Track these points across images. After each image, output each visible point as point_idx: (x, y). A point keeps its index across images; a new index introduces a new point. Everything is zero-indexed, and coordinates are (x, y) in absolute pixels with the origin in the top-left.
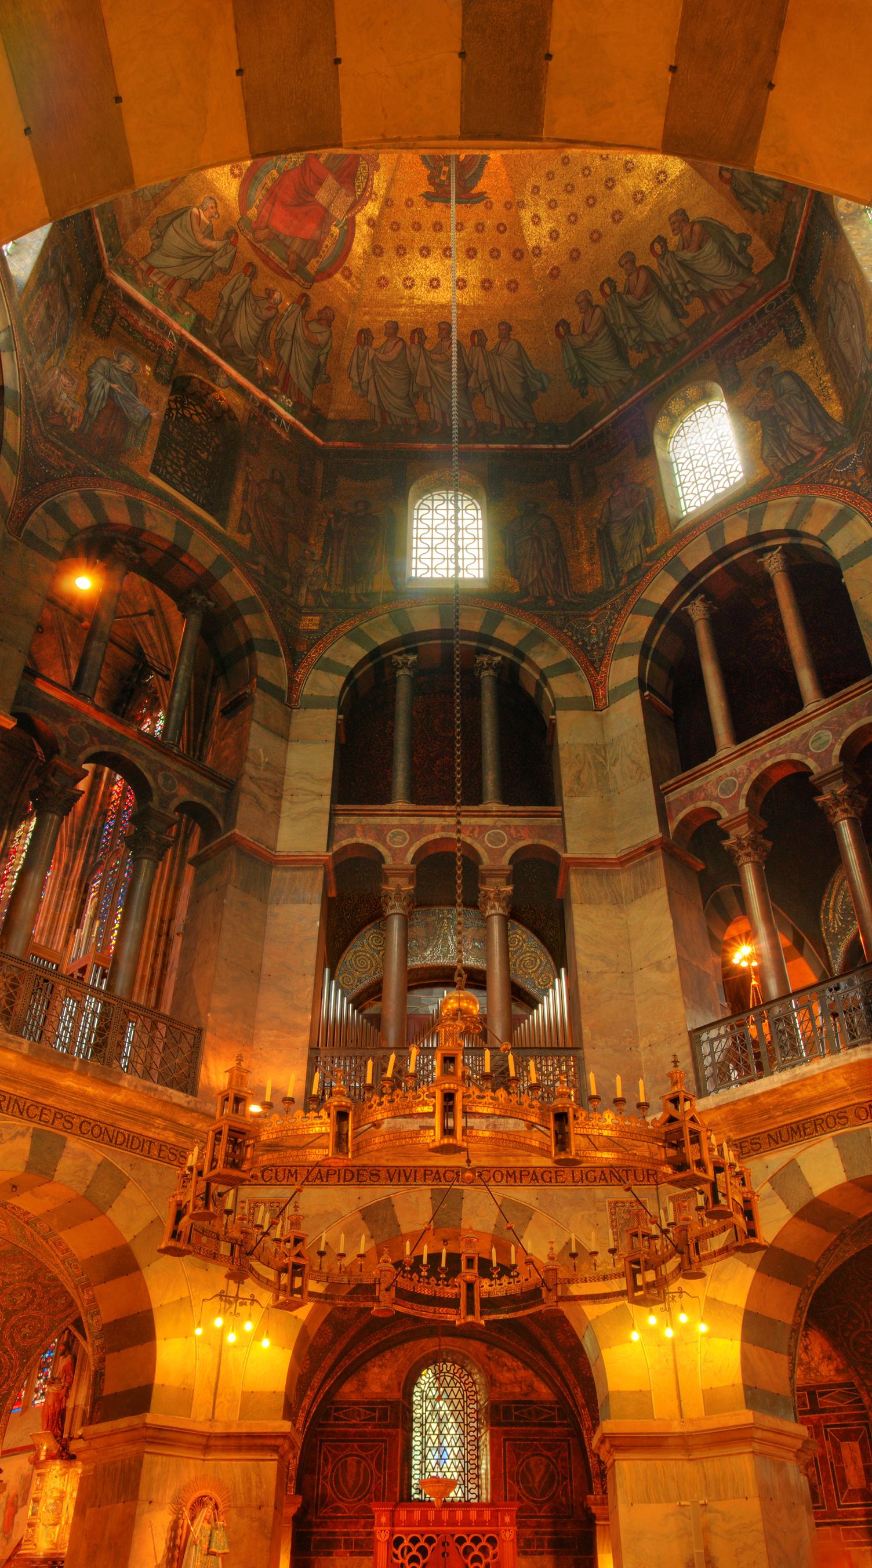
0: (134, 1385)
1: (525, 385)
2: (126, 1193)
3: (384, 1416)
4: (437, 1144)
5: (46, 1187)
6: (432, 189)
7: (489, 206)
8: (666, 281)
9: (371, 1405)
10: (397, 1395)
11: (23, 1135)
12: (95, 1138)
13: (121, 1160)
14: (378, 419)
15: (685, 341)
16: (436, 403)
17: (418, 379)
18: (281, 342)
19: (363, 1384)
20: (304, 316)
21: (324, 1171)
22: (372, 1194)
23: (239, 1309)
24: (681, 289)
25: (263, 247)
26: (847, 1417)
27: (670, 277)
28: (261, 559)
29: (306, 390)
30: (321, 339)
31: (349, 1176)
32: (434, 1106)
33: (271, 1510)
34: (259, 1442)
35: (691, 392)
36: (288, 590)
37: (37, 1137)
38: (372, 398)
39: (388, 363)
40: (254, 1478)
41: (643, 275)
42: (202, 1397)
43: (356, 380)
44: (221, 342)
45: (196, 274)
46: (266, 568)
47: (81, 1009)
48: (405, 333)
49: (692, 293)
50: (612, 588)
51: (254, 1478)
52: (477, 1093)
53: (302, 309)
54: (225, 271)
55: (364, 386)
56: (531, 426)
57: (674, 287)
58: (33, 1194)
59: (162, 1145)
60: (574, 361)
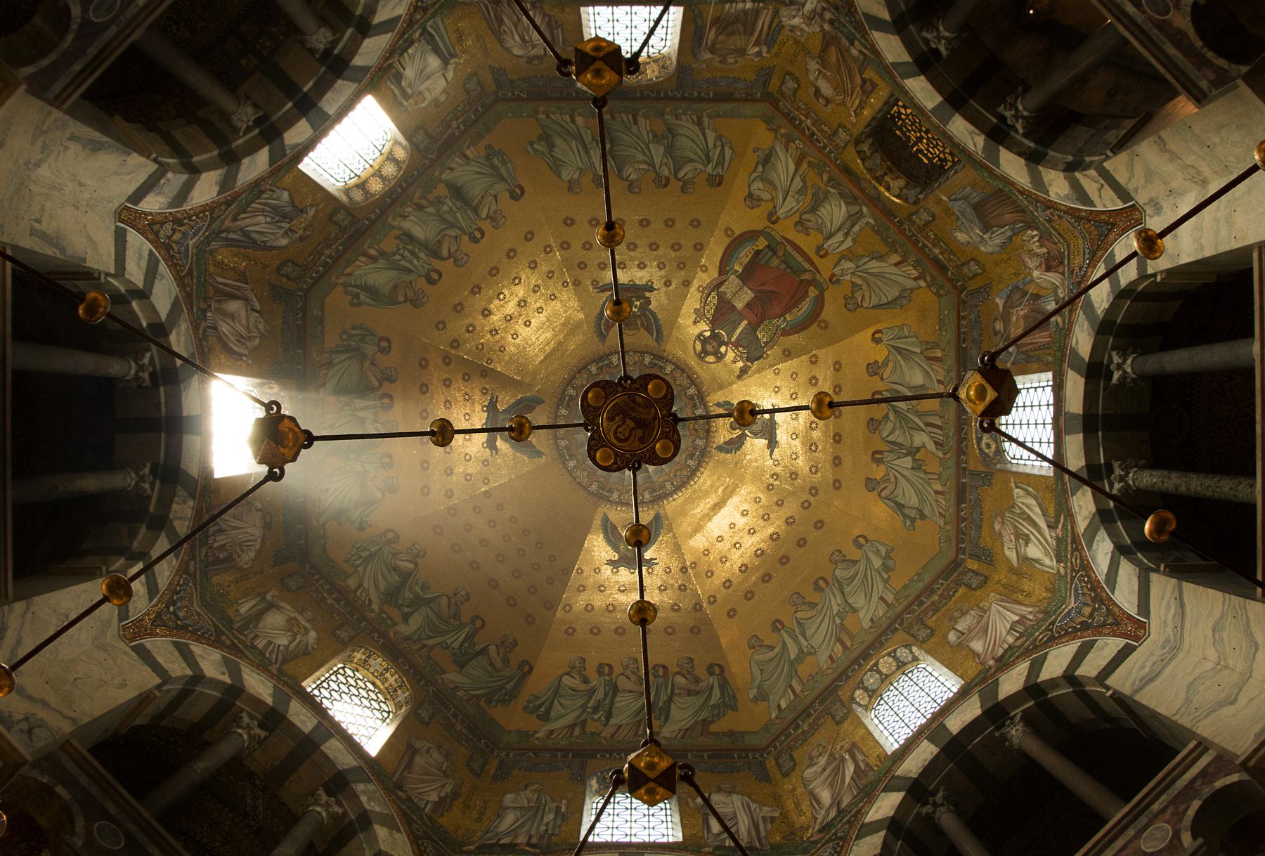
1: (551, 146)
6: (648, 294)
7: (595, 283)
8: (422, 255)
14: (706, 120)
15: (394, 220)
16: (644, 133)
17: (662, 149)
18: (801, 192)
20: (775, 207)
24: (407, 254)
25: (807, 266)
27: (418, 258)
28: (855, 52)
29: (779, 150)
30: (758, 185)
35: (376, 186)
36: (828, 16)
38: (711, 136)
39: (693, 161)
41: (445, 253)
43: (726, 149)
44: (861, 210)
45: (874, 263)
46: (852, 44)
48: (675, 185)
49: (394, 254)
50: (430, 23)
53: (776, 212)
54: (843, 257)
55: (719, 143)
56: (542, 116)
57: (413, 253)
60: (503, 171)
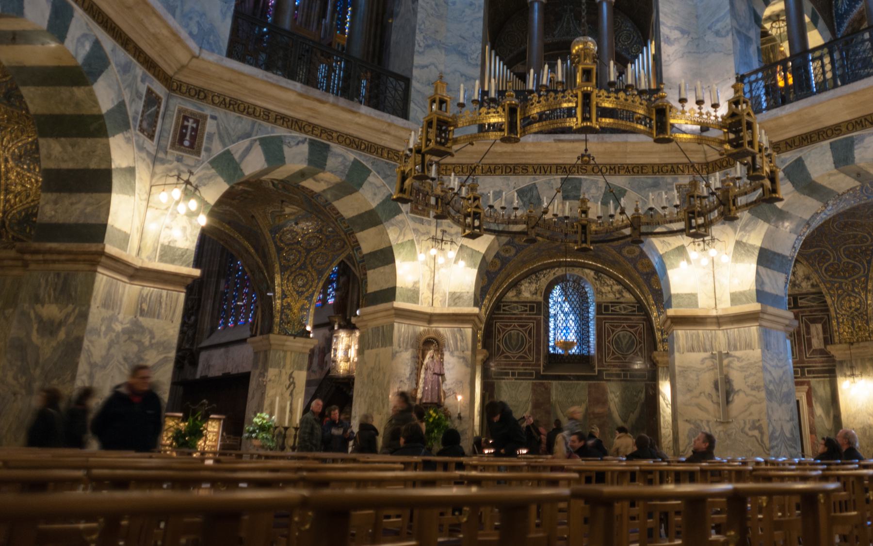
0: (385, 287)
2: (371, 179)
3: (532, 309)
4: (579, 126)
5: (321, 175)
9: (524, 303)
10: (540, 299)
11: (303, 142)
12: (348, 145)
13: (366, 160)
19: (519, 293)
21: (492, 167)
22: (525, 181)
23: (444, 246)
26: (816, 311)
31: (508, 170)
32: (577, 103)
33: (469, 353)
34: (461, 318)
37: (312, 143)
40: (458, 336)
42: (425, 293)
47: (331, 70)
51: (458, 336)
52: (606, 94)
58: (315, 180)
59: (390, 150)
